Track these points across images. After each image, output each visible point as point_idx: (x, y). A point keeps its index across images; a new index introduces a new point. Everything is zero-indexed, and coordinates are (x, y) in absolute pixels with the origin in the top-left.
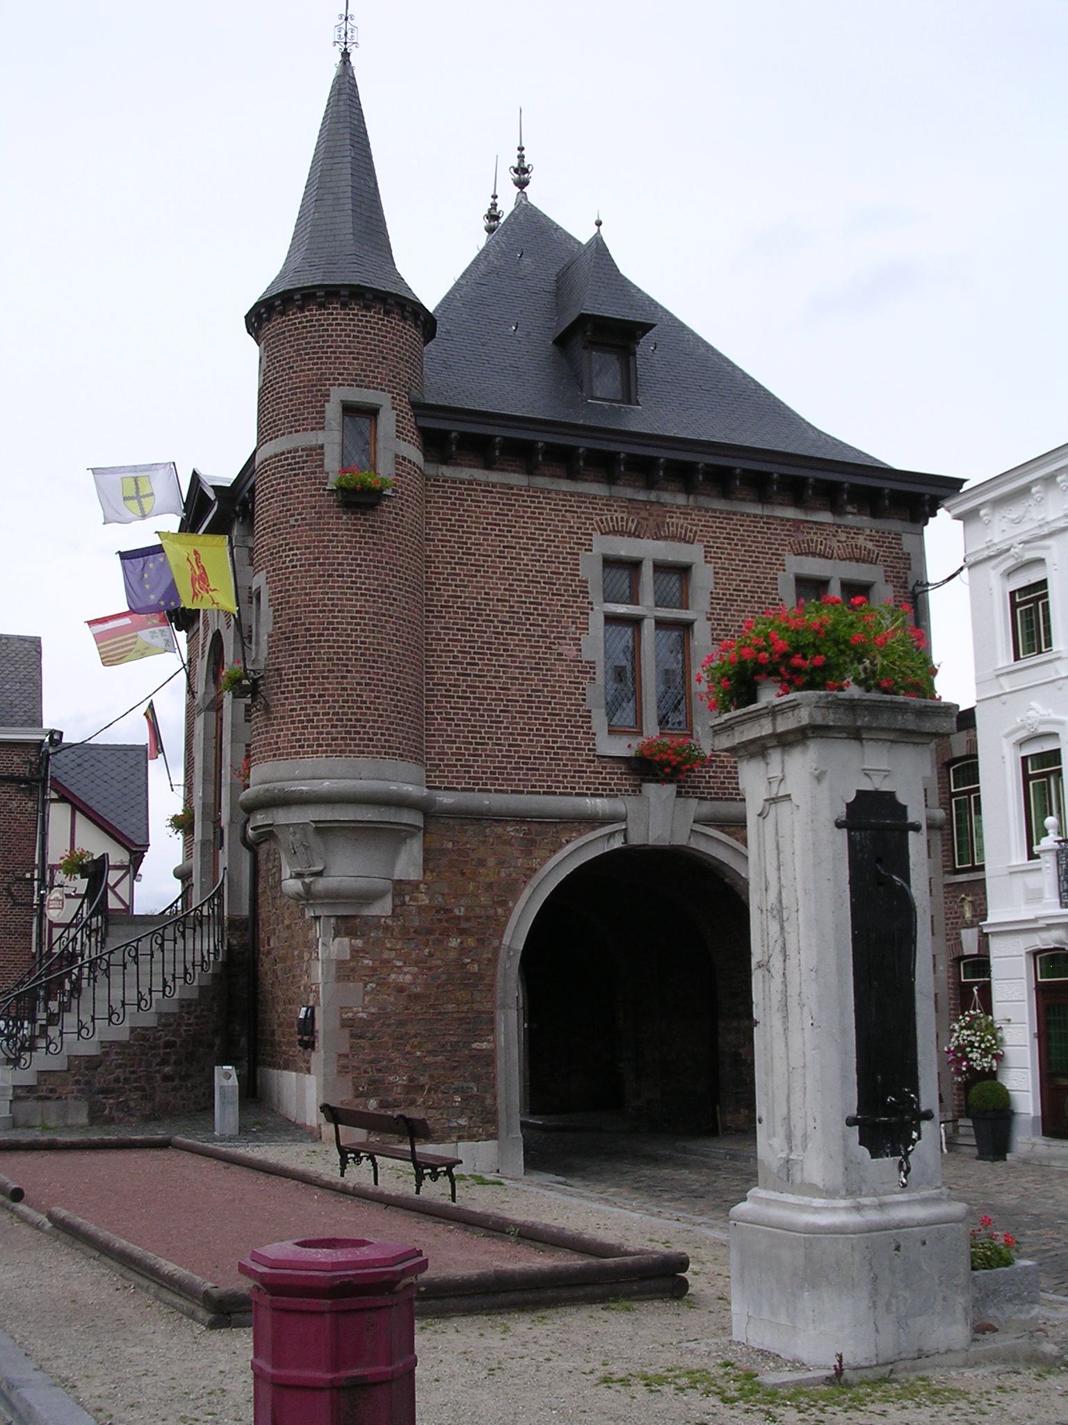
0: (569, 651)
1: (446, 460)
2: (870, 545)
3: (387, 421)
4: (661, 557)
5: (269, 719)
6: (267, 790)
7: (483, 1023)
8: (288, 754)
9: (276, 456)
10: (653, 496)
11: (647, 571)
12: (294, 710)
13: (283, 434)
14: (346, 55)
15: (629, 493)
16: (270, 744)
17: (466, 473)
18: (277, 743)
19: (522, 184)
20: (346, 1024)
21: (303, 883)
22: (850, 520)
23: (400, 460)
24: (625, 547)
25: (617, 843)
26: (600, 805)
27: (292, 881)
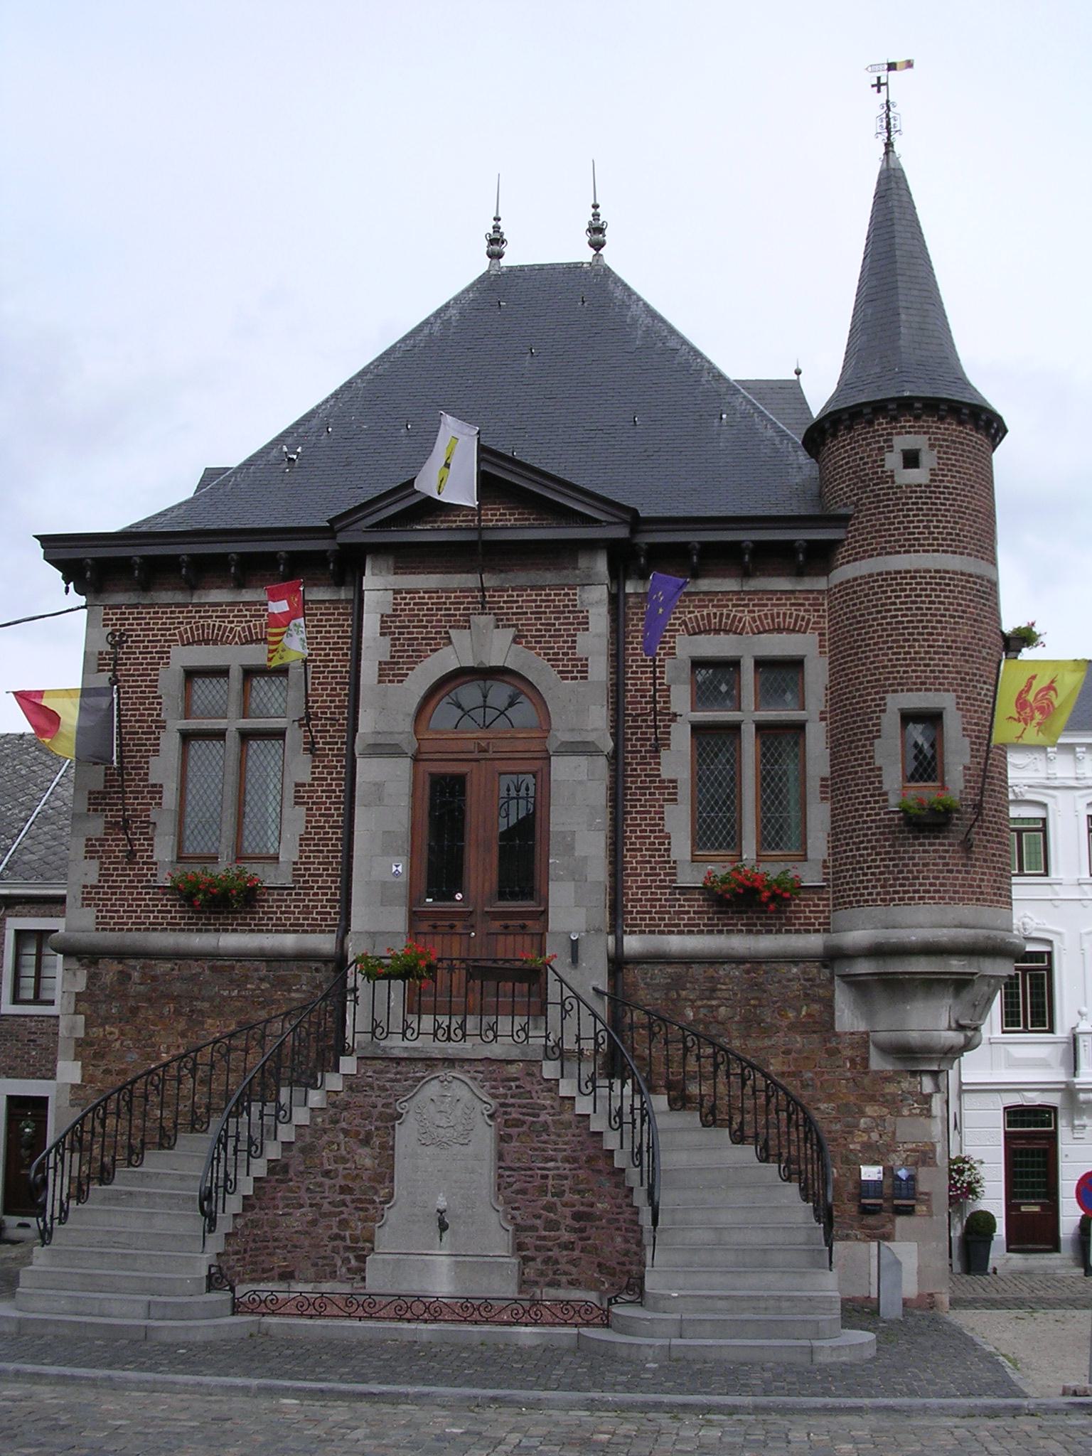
5: (971, 859)
6: (989, 938)
8: (992, 901)
9: (962, 574)
12: (994, 855)
13: (969, 555)
14: (889, 145)
16: (971, 886)
18: (980, 887)
19: (597, 246)
21: (966, 1036)
27: (951, 1034)
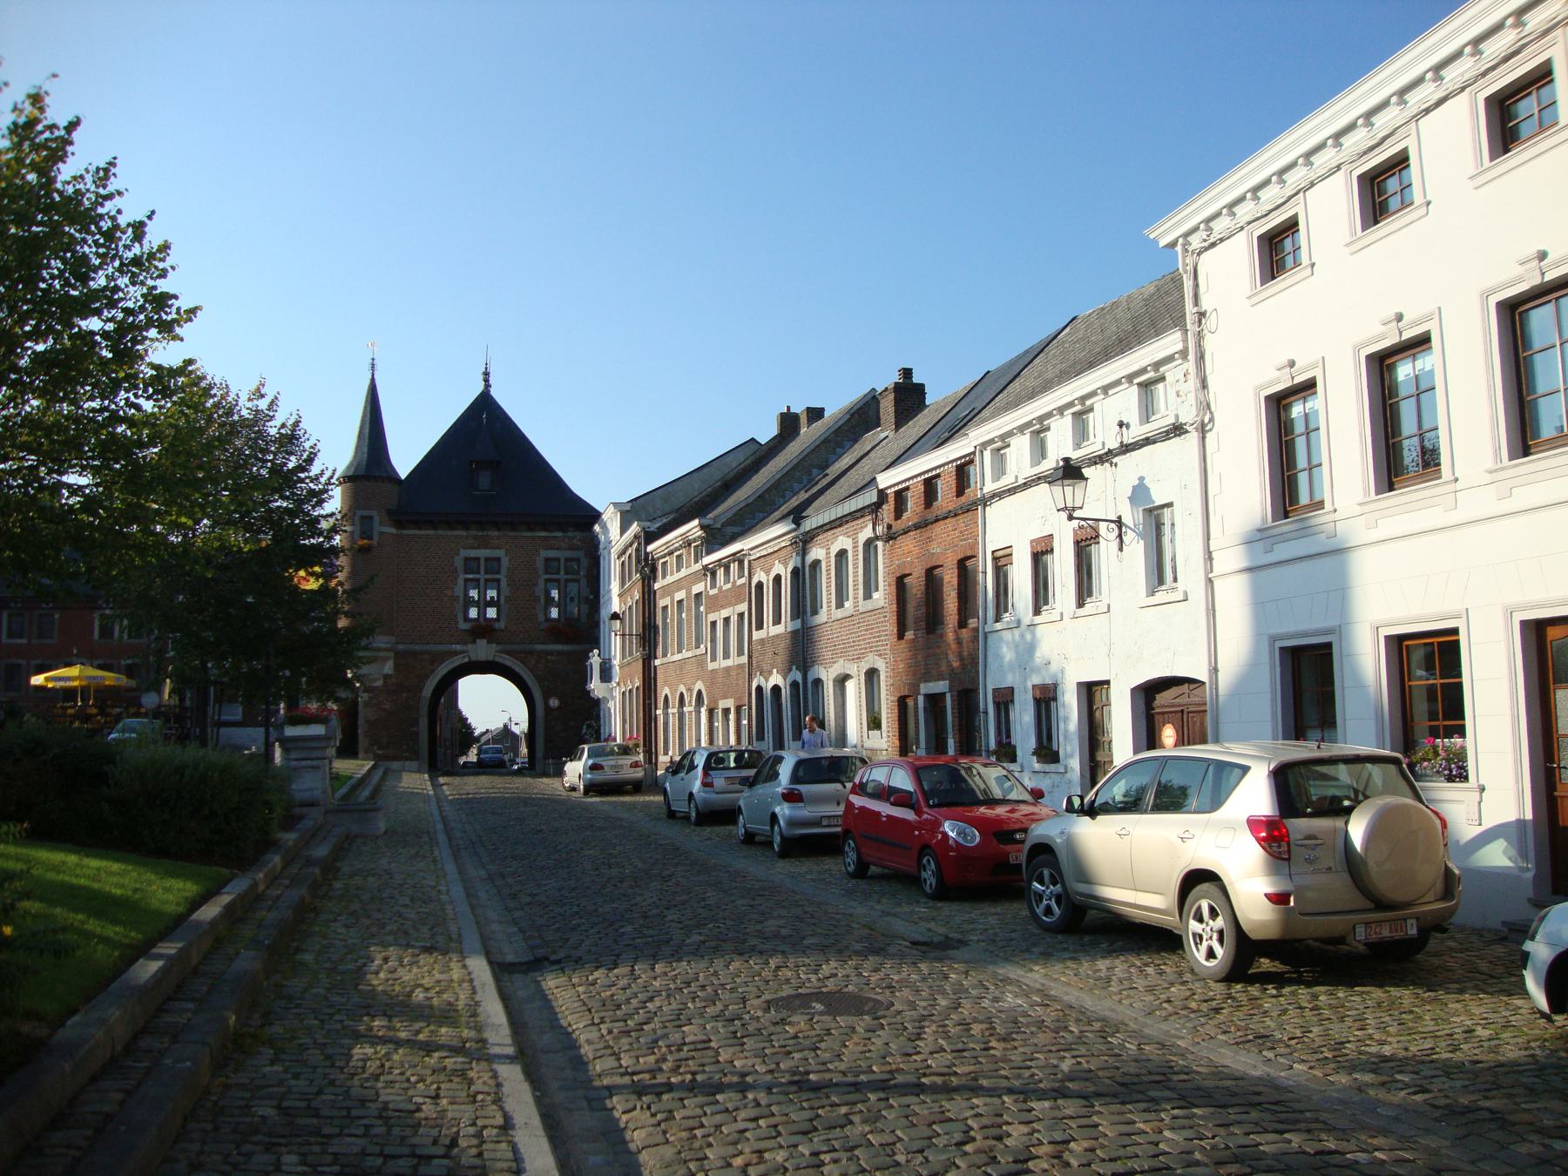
0: (449, 593)
1: (404, 528)
2: (579, 543)
3: (377, 519)
4: (488, 556)
7: (415, 722)
10: (485, 533)
11: (482, 563)
14: (373, 375)
15: (474, 532)
17: (412, 532)
20: (367, 721)
22: (570, 534)
23: (381, 533)
24: (473, 553)
25: (466, 660)
26: (458, 647)
